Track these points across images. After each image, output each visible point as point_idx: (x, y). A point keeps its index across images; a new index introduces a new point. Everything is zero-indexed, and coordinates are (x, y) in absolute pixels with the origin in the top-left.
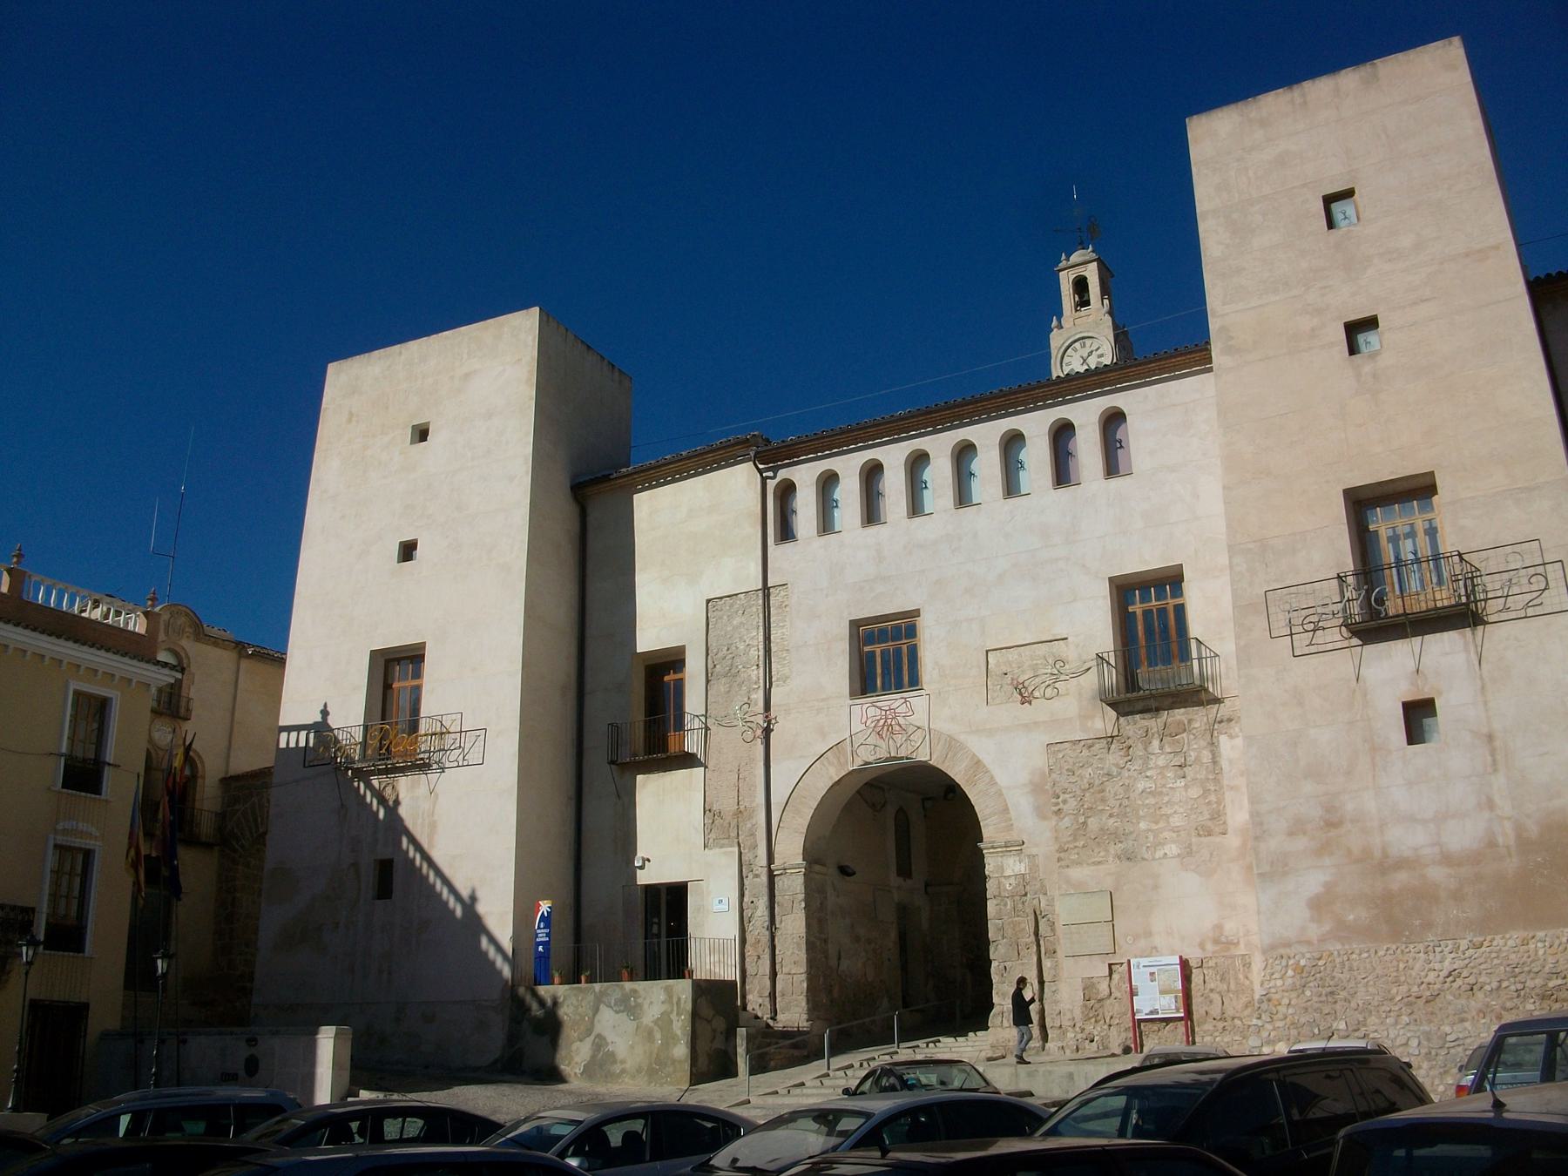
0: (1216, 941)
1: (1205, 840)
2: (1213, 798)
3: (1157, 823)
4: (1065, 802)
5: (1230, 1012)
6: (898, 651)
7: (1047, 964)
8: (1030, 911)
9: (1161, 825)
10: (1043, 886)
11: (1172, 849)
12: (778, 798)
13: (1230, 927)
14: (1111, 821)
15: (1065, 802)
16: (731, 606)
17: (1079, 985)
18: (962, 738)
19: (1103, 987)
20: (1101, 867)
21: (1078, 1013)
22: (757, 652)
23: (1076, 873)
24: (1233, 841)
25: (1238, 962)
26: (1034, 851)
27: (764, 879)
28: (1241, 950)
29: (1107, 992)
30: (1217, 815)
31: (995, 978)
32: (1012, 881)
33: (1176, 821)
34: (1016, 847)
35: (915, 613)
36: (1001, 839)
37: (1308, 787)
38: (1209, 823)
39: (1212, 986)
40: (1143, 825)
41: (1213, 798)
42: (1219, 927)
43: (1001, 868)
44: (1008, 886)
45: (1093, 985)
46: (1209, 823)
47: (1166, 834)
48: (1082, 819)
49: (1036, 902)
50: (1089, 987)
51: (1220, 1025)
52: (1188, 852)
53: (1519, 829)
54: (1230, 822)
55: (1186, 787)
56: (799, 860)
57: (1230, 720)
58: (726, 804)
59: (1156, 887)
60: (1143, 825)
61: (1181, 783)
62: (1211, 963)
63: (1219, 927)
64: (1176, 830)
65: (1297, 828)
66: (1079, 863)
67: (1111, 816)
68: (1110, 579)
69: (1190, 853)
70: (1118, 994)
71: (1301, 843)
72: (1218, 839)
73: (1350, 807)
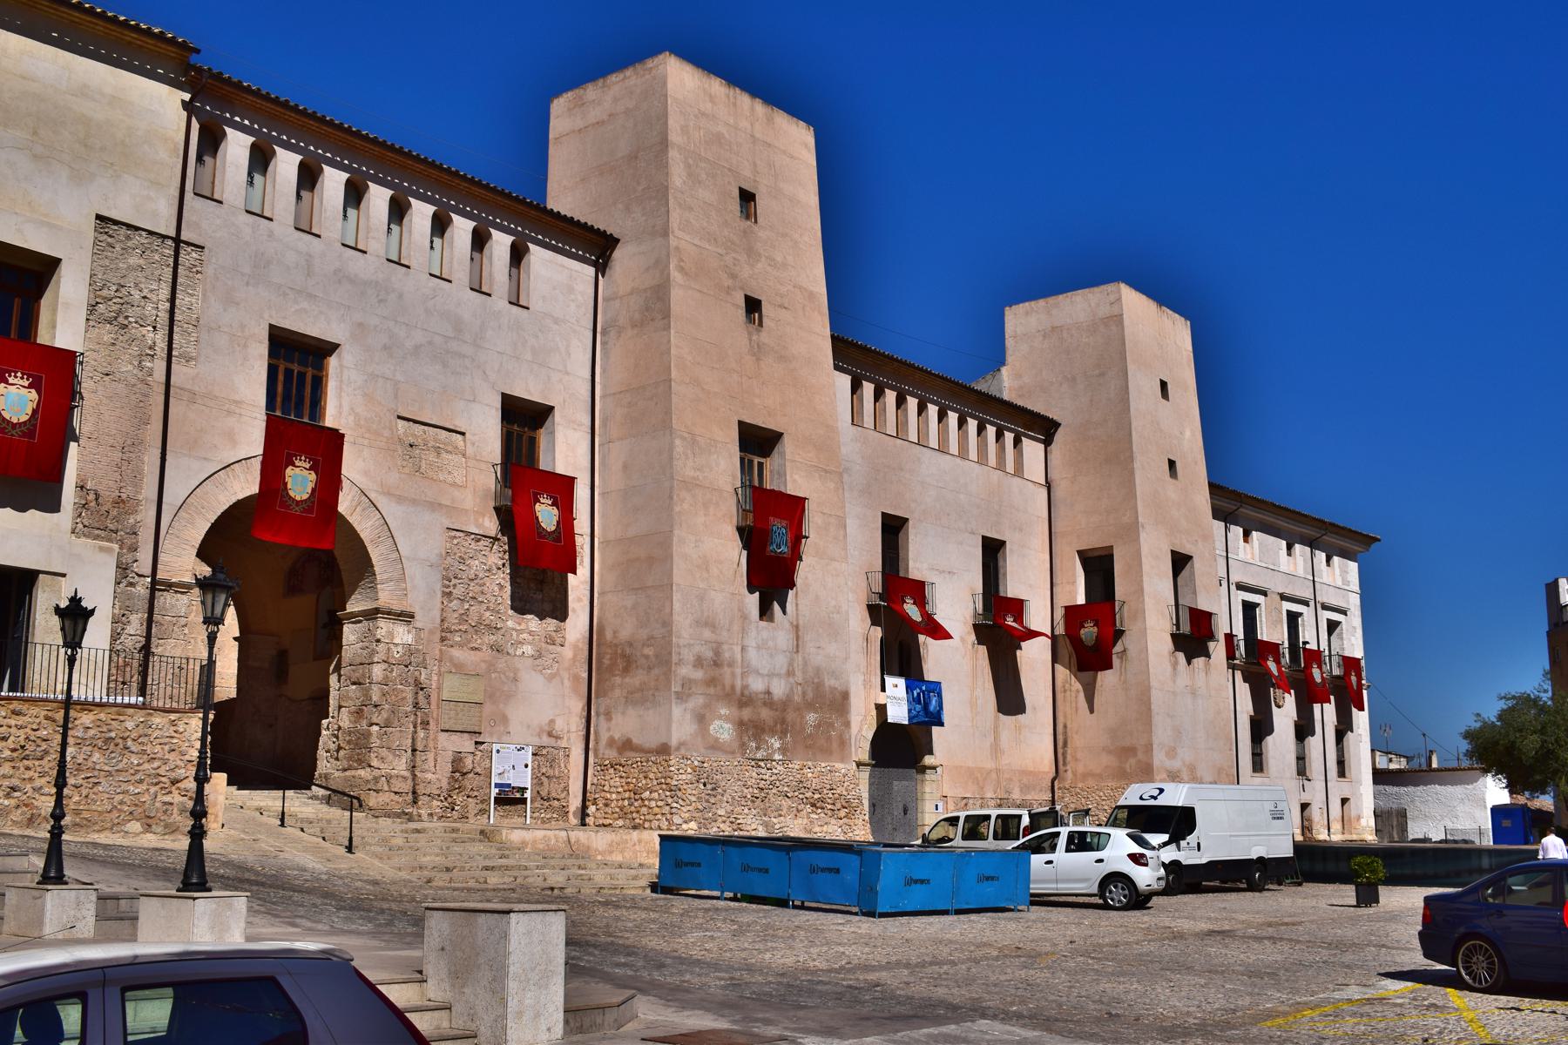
0: (550, 735)
6: (302, 376)
7: (421, 734)
8: (411, 681)
11: (528, 649)
12: (173, 496)
16: (128, 238)
17: (449, 756)
18: (372, 496)
19: (468, 762)
23: (457, 653)
24: (568, 653)
26: (419, 625)
27: (142, 589)
28: (563, 744)
31: (375, 741)
34: (406, 617)
37: (707, 634)
42: (552, 722)
43: (391, 634)
44: (397, 653)
45: (461, 759)
47: (525, 636)
50: (457, 760)
52: (539, 655)
53: (804, 693)
55: (543, 600)
59: (515, 680)
60: (510, 624)
61: (539, 596)
63: (552, 722)
64: (530, 633)
65: (699, 662)
66: (461, 645)
69: (540, 656)
70: (478, 770)
71: (699, 675)
72: (559, 649)
73: (727, 655)
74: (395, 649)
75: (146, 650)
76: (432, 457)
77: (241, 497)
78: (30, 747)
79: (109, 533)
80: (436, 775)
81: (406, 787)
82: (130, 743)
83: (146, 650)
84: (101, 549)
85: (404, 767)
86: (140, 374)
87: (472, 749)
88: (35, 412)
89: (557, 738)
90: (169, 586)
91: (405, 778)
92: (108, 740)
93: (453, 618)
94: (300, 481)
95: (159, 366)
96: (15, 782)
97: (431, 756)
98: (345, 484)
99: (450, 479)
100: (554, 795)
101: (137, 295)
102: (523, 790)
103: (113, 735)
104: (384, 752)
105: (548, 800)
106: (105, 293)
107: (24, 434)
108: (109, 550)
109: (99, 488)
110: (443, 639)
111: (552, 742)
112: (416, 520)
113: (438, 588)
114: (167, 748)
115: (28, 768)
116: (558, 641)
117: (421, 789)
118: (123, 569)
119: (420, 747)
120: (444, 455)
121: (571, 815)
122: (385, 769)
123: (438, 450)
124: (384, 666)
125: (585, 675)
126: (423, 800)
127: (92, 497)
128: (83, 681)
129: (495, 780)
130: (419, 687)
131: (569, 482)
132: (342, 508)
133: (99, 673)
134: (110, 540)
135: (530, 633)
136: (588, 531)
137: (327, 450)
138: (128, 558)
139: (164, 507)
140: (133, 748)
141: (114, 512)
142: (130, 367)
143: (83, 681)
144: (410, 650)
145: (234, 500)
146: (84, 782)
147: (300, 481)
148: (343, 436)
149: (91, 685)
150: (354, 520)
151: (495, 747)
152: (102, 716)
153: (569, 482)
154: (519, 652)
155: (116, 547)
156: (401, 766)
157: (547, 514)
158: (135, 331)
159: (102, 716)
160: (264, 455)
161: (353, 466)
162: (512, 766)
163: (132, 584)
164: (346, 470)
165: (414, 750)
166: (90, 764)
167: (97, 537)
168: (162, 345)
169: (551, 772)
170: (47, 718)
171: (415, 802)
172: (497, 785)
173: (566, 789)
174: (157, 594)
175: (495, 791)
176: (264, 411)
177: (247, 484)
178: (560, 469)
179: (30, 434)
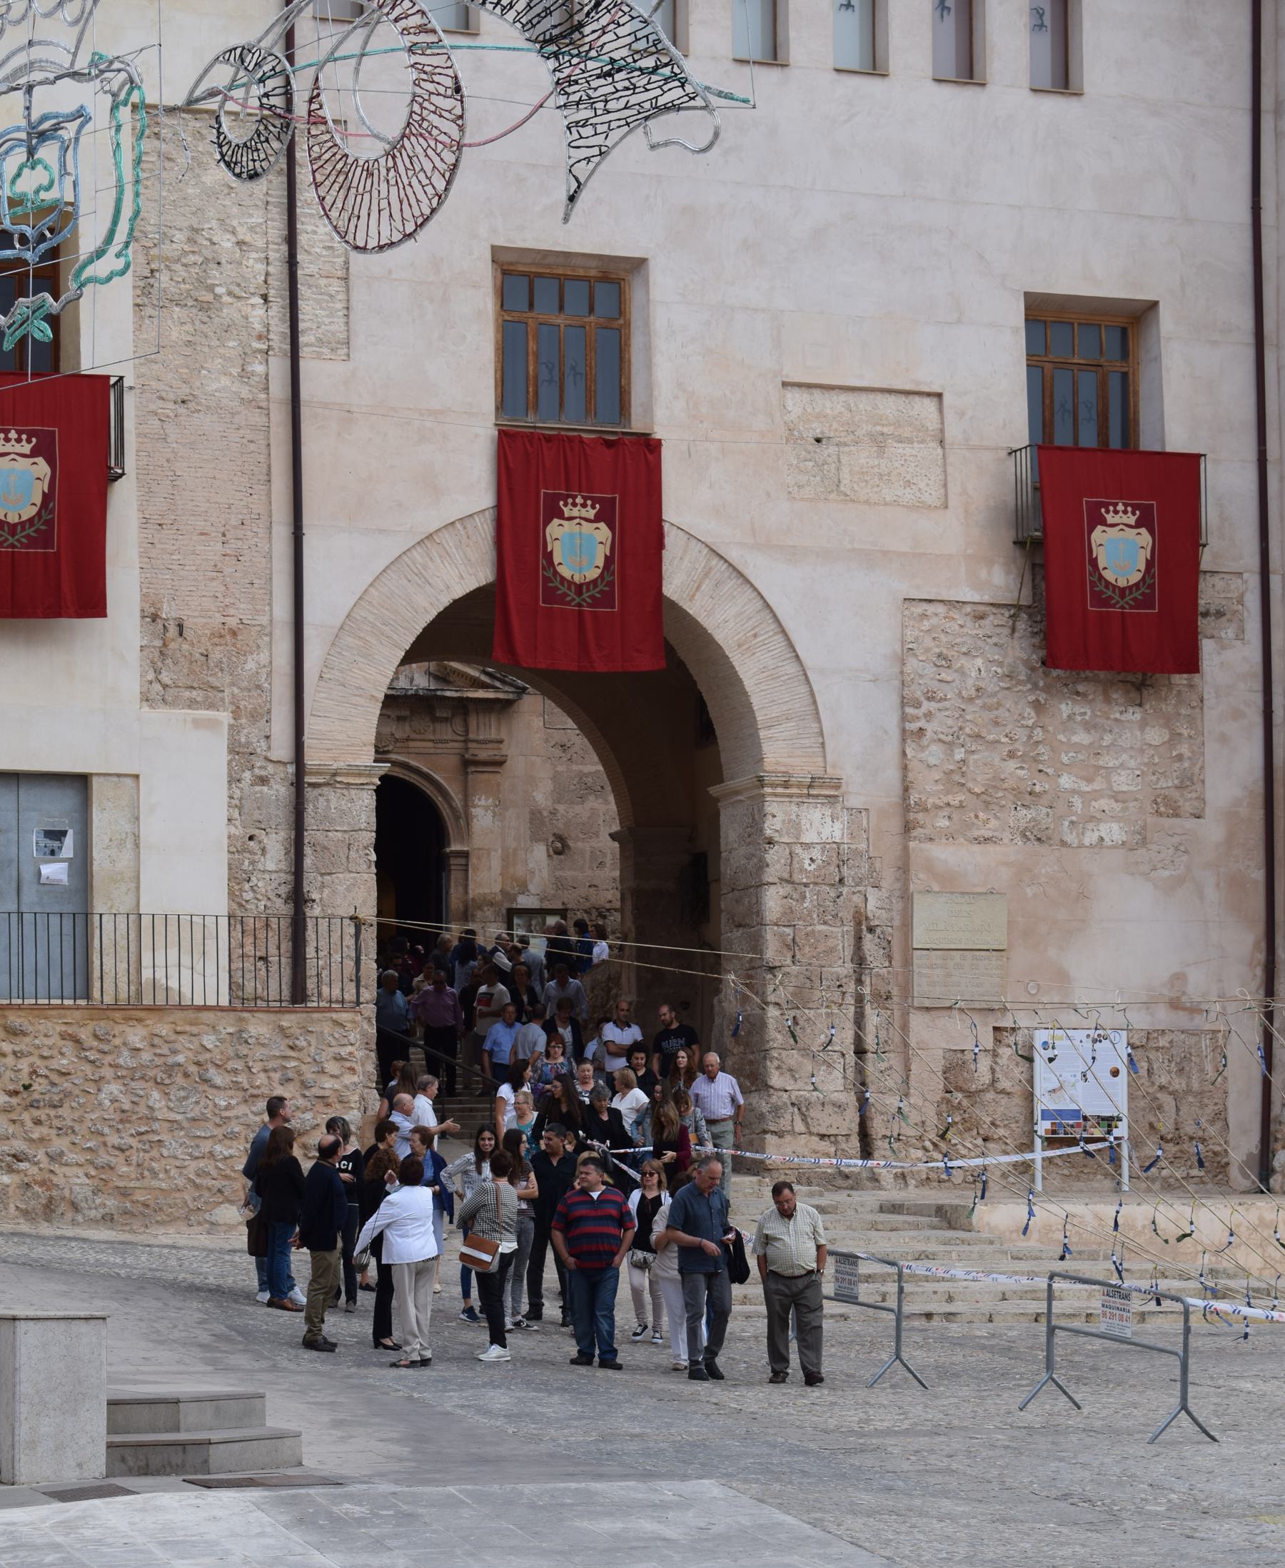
0: (1175, 1005)
1: (1168, 822)
2: (1184, 749)
3: (1089, 780)
4: (929, 716)
5: (1189, 1129)
7: (873, 1019)
8: (847, 915)
9: (1098, 785)
10: (872, 869)
11: (1113, 832)
13: (1198, 984)
14: (1012, 764)
15: (929, 716)
18: (733, 555)
20: (990, 848)
21: (932, 1120)
22: (261, 265)
23: (945, 854)
24: (1212, 831)
25: (1205, 1042)
26: (854, 801)
27: (280, 791)
29: (987, 1079)
30: (1188, 781)
31: (776, 1037)
32: (816, 853)
33: (1122, 782)
34: (822, 789)
35: (638, 265)
36: (803, 767)
38: (1176, 794)
39: (1163, 1080)
40: (1066, 781)
41: (1184, 749)
43: (795, 826)
44: (808, 863)
46: (1176, 794)
47: (1104, 803)
48: (959, 754)
49: (857, 899)
51: (1172, 1149)
54: (1209, 795)
56: (366, 757)
57: (1220, 614)
58: (198, 608)
60: (1066, 781)
62: (1163, 1042)
63: (1179, 977)
64: (1116, 796)
66: (951, 836)
67: (1011, 755)
68: (1027, 294)
69: (1144, 842)
70: (1004, 1084)
72: (1191, 823)
74: (805, 856)
75: (298, 898)
76: (863, 457)
77: (459, 592)
78: (39, 1086)
79: (208, 695)
80: (909, 1102)
81: (850, 1121)
82: (212, 1073)
83: (298, 898)
84: (197, 723)
85: (840, 1083)
86: (245, 392)
87: (988, 1041)
88: (47, 498)
89: (1194, 1010)
90: (333, 779)
91: (839, 1106)
92: (170, 1069)
93: (928, 787)
94: (579, 545)
95: (278, 368)
96: (19, 1145)
97: (894, 1060)
98: (672, 539)
99: (908, 495)
100: (1189, 1129)
101: (227, 243)
102: (1109, 1122)
103: (180, 1058)
104: (793, 1058)
105: (1177, 1141)
106: (167, 249)
107: (32, 542)
108: (212, 724)
109: (184, 614)
110: (907, 828)
111: (1181, 1020)
112: (838, 590)
113: (892, 722)
114: (276, 1076)
115: (38, 1122)
116: (1187, 807)
117: (878, 1127)
118: (240, 753)
119: (870, 1042)
120: (895, 448)
121: (1234, 1172)
122: (800, 1090)
123: (879, 442)
124: (788, 888)
125: (1259, 875)
126: (880, 1146)
127: (173, 631)
128: (186, 960)
129: (1044, 1102)
130: (862, 925)
131: (1190, 464)
132: (675, 585)
133: (211, 945)
134: (211, 706)
135: (1116, 796)
136: (1254, 562)
137: (626, 476)
138: (250, 734)
139: (308, 632)
140: (218, 1081)
141: (216, 654)
142: (225, 381)
143: (186, 960)
144: (839, 856)
145: (445, 601)
146: (133, 1142)
147: (579, 545)
148: (659, 442)
149: (199, 967)
150: (696, 608)
151: (1040, 1037)
152: (164, 1030)
153: (1190, 464)
154: (1091, 838)
155: (225, 717)
156: (834, 1082)
157: (1121, 550)
158: (230, 311)
159: (164, 1030)
160: (499, 507)
161: (686, 501)
162: (1082, 1077)
163: (263, 781)
164: (673, 511)
165: (860, 1052)
166: (143, 1110)
167: (192, 704)
168: (280, 329)
169: (1178, 1084)
170: (63, 1036)
171: (866, 1153)
172: (1046, 1115)
173: (1220, 1116)
174: (310, 793)
175: (1043, 1127)
176: (492, 419)
177: (466, 570)
178: (1177, 440)
179: (44, 539)
